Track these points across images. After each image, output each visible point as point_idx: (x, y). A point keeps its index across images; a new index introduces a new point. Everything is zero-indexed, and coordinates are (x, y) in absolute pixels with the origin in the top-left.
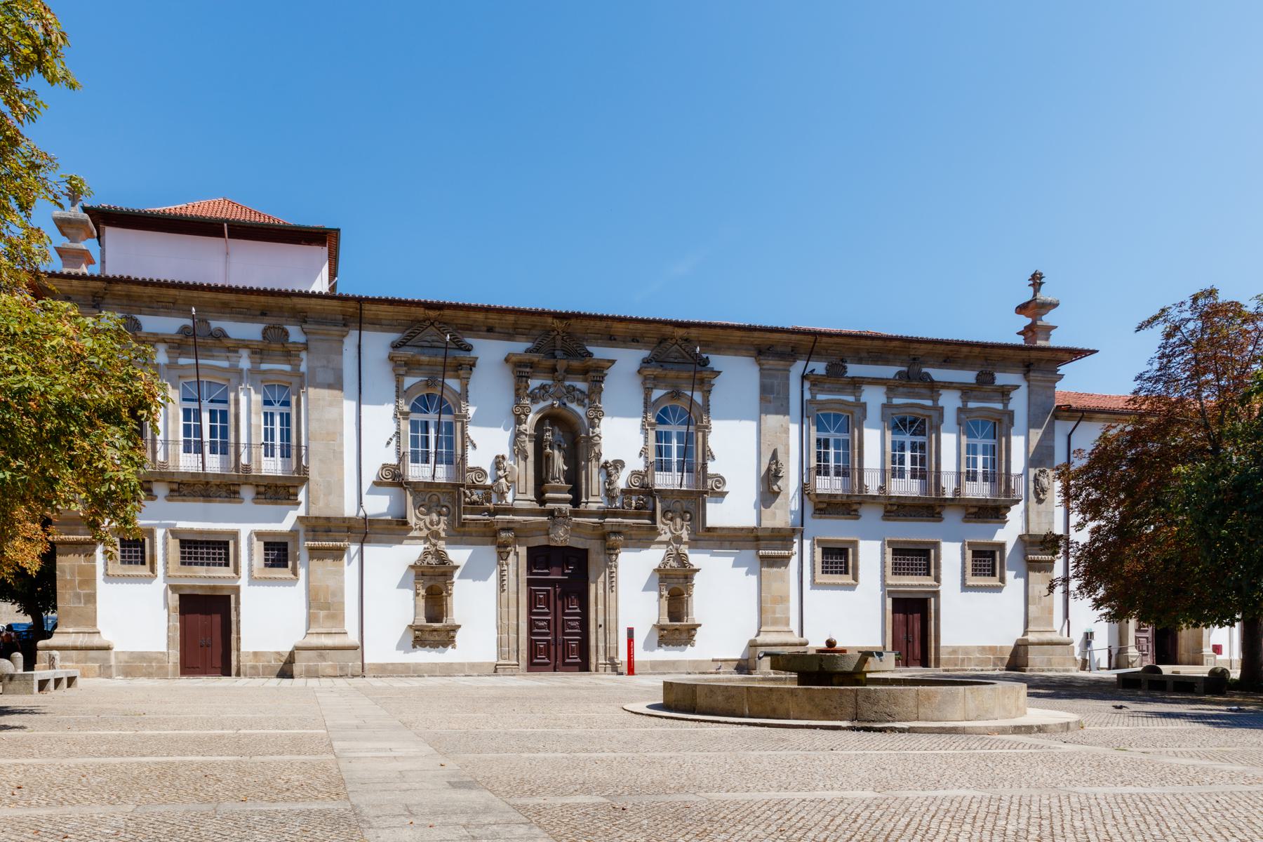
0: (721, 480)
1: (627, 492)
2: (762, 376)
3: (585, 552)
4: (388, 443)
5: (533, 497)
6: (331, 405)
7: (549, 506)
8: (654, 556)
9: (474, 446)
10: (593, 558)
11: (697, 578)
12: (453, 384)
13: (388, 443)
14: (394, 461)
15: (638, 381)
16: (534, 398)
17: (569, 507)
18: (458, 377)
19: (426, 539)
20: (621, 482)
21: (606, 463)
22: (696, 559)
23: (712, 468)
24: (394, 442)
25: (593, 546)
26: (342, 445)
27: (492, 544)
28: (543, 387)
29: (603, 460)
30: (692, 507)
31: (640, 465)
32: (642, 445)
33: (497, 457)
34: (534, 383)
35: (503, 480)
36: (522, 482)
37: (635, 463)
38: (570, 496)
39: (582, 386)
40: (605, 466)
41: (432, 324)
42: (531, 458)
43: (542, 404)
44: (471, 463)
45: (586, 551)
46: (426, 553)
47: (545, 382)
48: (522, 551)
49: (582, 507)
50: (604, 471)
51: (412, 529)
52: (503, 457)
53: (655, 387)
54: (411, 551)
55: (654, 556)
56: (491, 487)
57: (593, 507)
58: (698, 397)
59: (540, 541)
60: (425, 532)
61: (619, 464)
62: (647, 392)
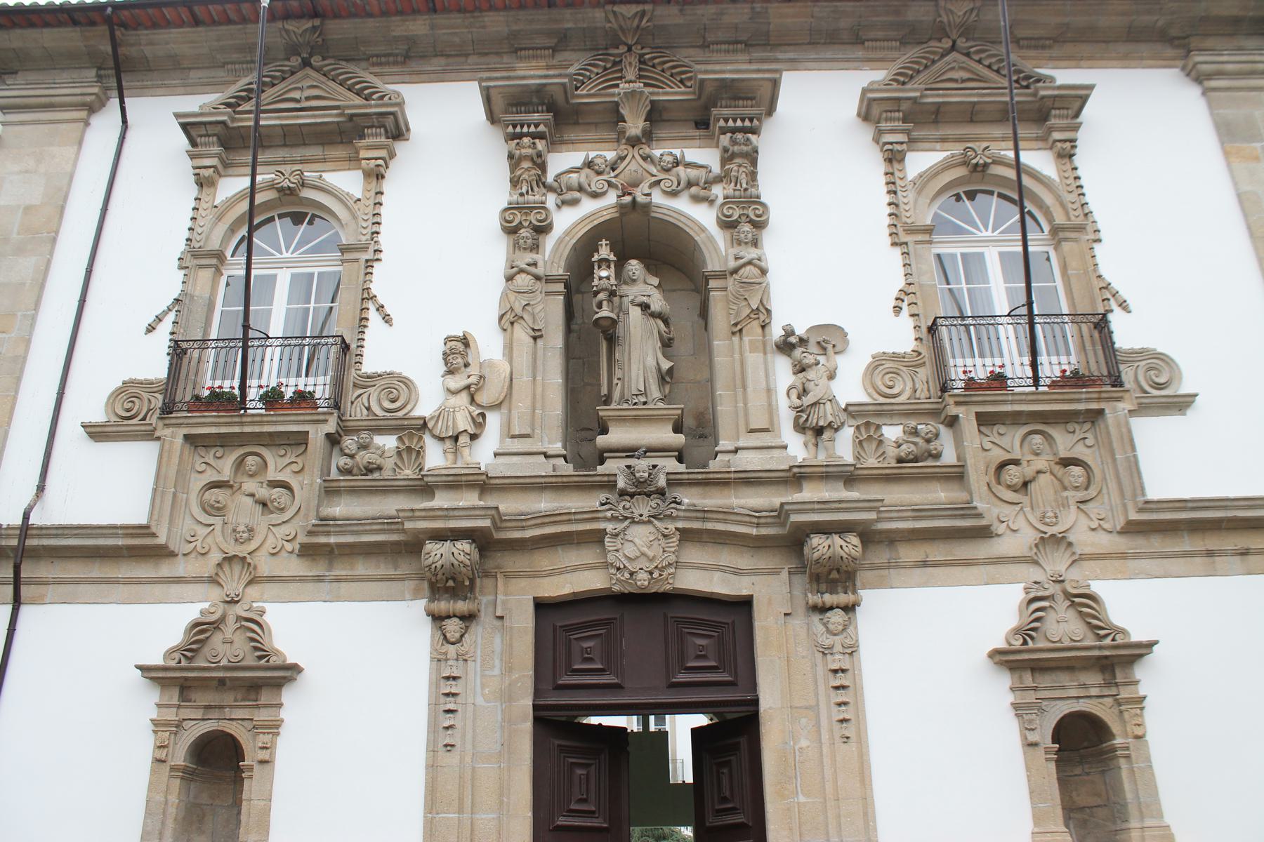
0: (1156, 360)
1: (866, 418)
2: (1211, 106)
3: (744, 605)
4: (151, 329)
5: (557, 447)
6: (20, 250)
7: (613, 466)
8: (986, 609)
9: (387, 319)
10: (765, 623)
11: (1149, 679)
12: (348, 182)
13: (151, 329)
14: (158, 369)
15: (865, 134)
16: (569, 194)
17: (670, 465)
18: (353, 161)
19: (214, 581)
20: (849, 386)
21: (789, 332)
22: (1134, 602)
23: (1125, 333)
24: (166, 326)
25: (771, 592)
26: (28, 342)
27: (416, 595)
28: (589, 164)
29: (777, 332)
30: (1080, 452)
31: (901, 336)
32: (901, 283)
33: (448, 339)
34: (562, 162)
35: (464, 397)
36: (521, 405)
37: (879, 331)
38: (680, 439)
39: (705, 156)
40: (786, 346)
41: (306, 63)
42: (556, 338)
43: (588, 206)
44: (373, 361)
45: (744, 605)
46: (202, 630)
47: (592, 154)
48: (525, 620)
49: (714, 465)
50: (783, 373)
51: (162, 553)
52: (465, 341)
53: (912, 142)
54: (158, 624)
55: (986, 609)
56: (424, 425)
57: (750, 461)
58: (1038, 160)
59: (576, 576)
60: (216, 557)
61: (829, 339)
62: (894, 158)
